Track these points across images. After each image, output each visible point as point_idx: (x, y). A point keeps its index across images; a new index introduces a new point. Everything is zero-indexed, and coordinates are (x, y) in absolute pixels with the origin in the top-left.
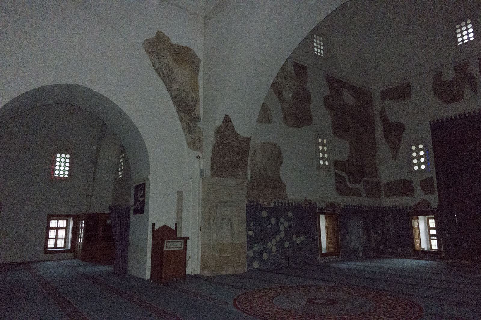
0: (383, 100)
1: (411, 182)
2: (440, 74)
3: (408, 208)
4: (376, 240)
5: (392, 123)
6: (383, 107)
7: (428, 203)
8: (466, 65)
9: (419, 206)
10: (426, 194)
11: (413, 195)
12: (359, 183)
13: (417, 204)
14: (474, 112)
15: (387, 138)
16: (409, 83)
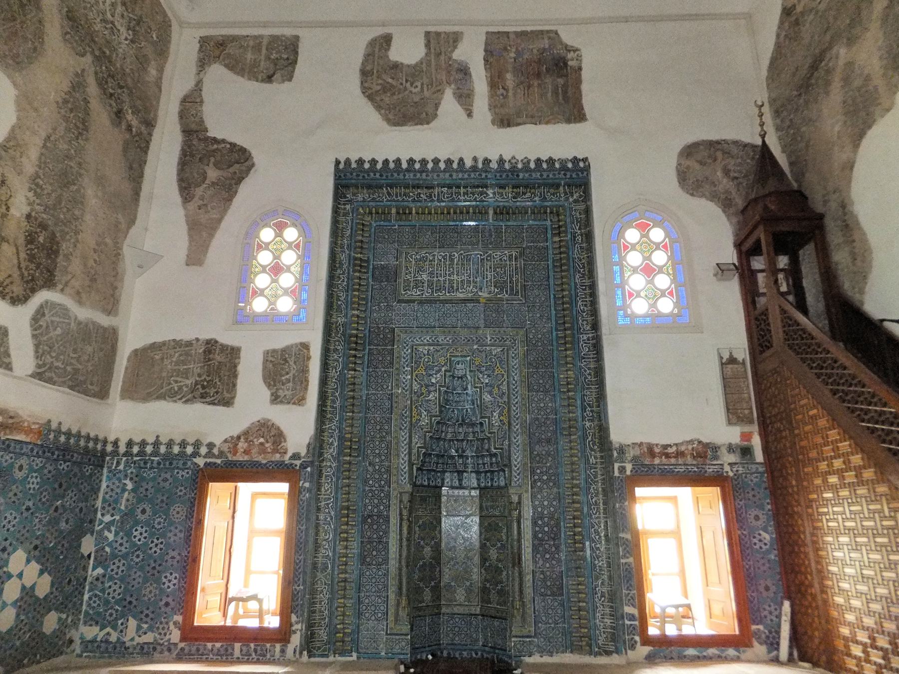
0: (202, 64)
1: (233, 353)
2: (386, 40)
3: (203, 450)
4: (28, 592)
5: (215, 140)
6: (199, 86)
7: (278, 437)
8: (455, 39)
9: (242, 445)
10: (276, 399)
11: (227, 403)
12: (16, 301)
13: (239, 438)
14: (461, 160)
15: (186, 186)
16: (297, 38)
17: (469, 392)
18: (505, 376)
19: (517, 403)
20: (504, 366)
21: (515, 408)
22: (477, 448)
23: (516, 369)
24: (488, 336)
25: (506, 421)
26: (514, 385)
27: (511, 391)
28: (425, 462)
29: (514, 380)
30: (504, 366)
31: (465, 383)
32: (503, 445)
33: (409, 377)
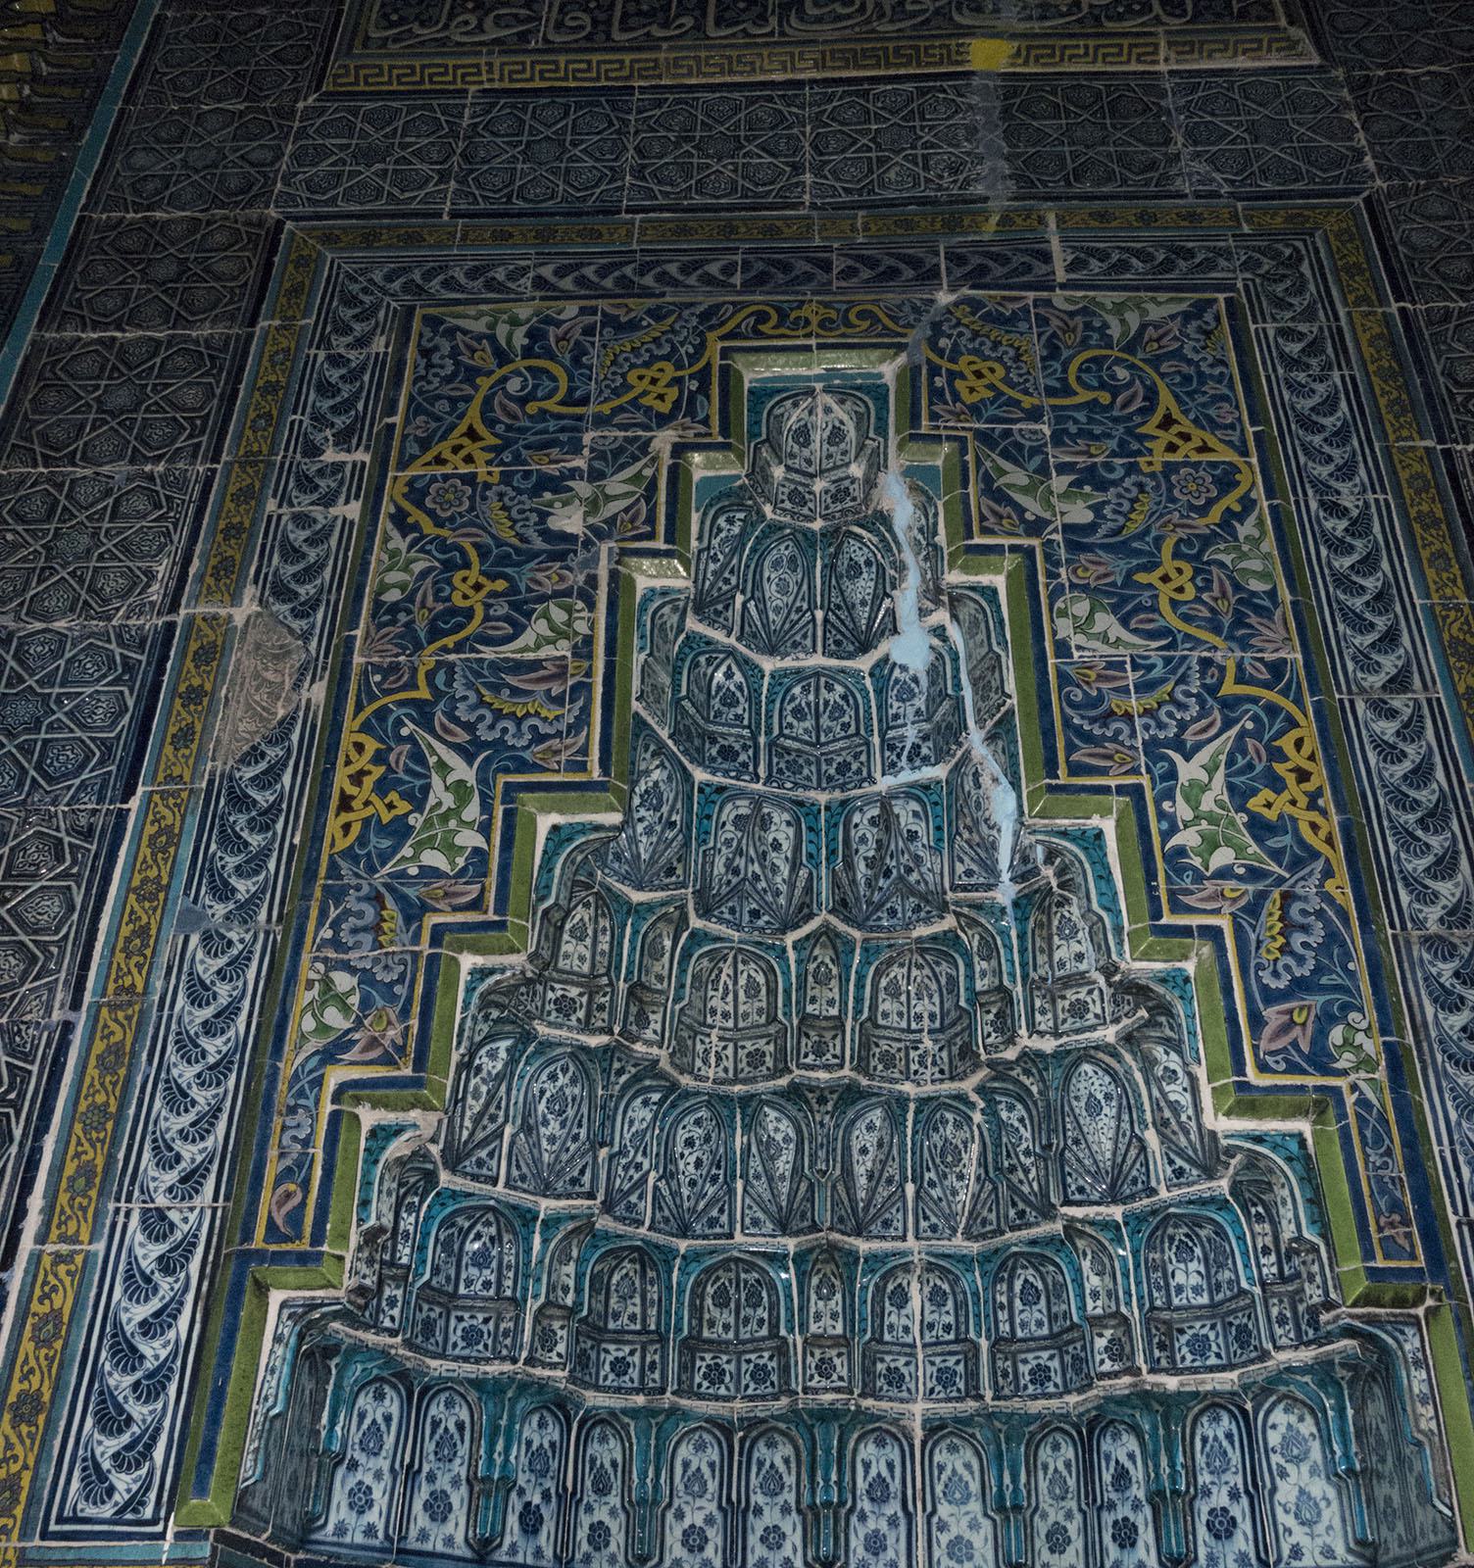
17: (910, 650)
18: (1251, 478)
19: (1399, 682)
20: (1224, 413)
21: (1387, 729)
22: (996, 1168)
23: (1341, 436)
24: (1055, 246)
25: (1320, 830)
26: (1340, 547)
27: (1324, 589)
28: (446, 1298)
29: (1335, 509)
30: (1224, 413)
31: (863, 587)
32: (1320, 1059)
33: (353, 510)
